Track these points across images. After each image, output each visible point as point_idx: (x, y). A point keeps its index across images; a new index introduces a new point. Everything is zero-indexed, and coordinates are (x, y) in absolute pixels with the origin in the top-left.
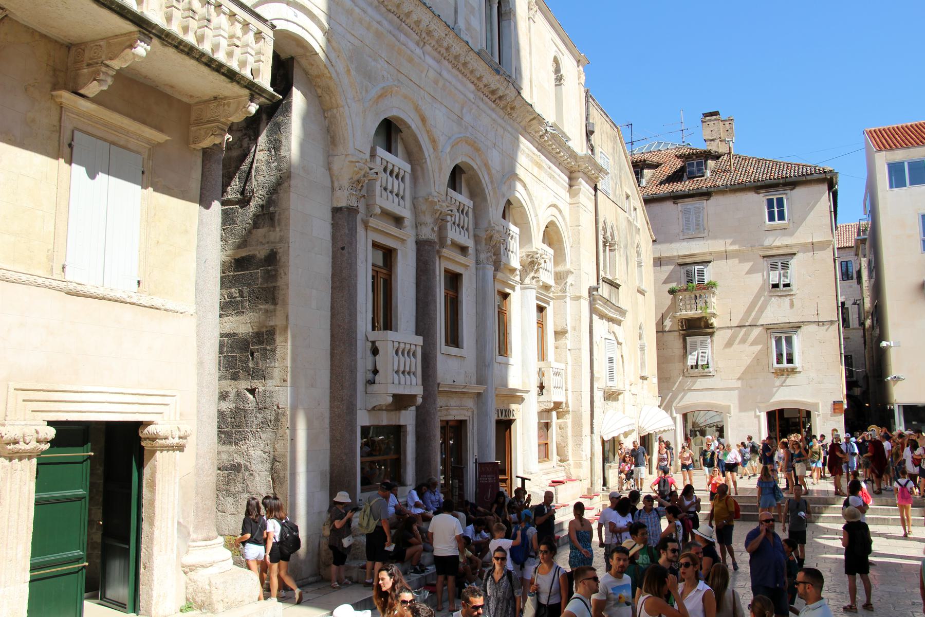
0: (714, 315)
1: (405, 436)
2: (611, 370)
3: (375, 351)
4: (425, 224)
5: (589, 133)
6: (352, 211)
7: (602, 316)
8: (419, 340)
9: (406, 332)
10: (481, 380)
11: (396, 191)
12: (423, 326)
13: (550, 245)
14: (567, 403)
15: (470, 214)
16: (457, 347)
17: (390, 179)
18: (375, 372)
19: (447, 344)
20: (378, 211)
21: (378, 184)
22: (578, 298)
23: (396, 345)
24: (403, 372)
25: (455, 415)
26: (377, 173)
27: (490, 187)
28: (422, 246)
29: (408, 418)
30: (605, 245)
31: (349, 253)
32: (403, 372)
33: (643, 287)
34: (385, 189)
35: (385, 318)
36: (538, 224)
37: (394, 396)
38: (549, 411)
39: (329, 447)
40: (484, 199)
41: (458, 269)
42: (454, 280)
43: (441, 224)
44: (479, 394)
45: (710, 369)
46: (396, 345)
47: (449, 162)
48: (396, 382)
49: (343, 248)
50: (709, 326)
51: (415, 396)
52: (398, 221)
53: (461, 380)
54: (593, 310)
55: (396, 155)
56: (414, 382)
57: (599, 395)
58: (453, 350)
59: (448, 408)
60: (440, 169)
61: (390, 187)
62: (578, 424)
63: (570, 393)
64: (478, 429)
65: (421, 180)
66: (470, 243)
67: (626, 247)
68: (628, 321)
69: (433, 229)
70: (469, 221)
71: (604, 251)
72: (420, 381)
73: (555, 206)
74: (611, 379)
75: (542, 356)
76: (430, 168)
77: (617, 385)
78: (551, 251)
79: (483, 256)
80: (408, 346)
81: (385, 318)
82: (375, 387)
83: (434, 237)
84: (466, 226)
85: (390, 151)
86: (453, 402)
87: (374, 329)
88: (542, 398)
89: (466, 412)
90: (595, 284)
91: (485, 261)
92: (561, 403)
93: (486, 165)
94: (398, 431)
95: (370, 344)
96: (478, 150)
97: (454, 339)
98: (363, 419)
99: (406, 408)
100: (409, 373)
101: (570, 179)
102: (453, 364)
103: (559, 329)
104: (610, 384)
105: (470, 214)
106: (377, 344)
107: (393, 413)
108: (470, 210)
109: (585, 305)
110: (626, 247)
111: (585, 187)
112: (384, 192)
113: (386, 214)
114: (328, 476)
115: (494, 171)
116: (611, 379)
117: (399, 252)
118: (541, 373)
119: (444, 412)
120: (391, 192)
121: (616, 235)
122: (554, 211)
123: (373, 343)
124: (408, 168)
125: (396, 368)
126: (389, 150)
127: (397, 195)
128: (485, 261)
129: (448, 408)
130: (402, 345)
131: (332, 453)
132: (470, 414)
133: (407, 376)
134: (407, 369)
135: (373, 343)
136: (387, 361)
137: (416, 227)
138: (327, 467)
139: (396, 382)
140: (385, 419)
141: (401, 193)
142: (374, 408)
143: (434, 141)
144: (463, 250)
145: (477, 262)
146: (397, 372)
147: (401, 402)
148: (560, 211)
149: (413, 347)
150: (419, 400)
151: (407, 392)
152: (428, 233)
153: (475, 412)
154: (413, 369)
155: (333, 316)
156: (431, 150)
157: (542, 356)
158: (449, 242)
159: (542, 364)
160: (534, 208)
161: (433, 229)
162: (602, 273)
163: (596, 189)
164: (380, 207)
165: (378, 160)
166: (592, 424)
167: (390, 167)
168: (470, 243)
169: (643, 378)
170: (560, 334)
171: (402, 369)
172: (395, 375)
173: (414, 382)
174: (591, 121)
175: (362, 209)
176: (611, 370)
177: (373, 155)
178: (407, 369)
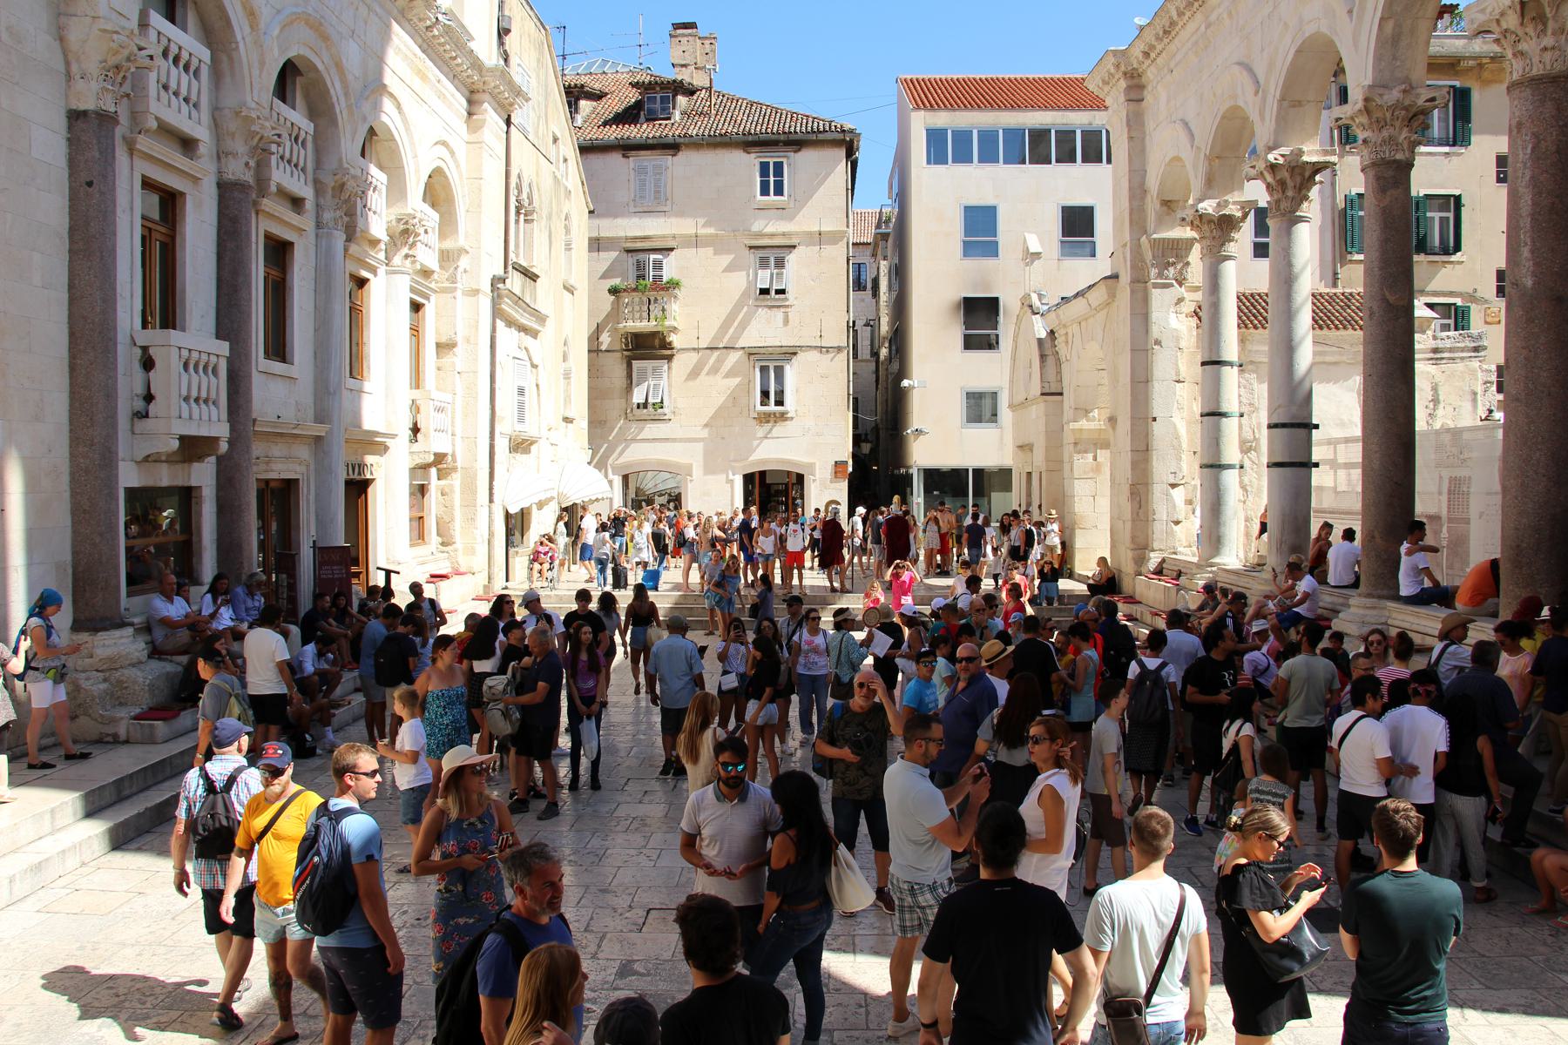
0: (674, 330)
1: (199, 504)
2: (521, 407)
3: (148, 364)
4: (235, 155)
5: (503, 32)
6: (105, 120)
7: (510, 323)
8: (224, 348)
9: (198, 332)
10: (321, 417)
11: (184, 92)
12: (229, 324)
13: (433, 206)
14: (453, 456)
15: (310, 145)
16: (283, 360)
17: (173, 69)
18: (149, 398)
19: (267, 355)
20: (154, 125)
21: (153, 76)
22: (476, 292)
23: (185, 353)
24: (197, 400)
25: (280, 471)
26: (151, 57)
27: (343, 104)
28: (228, 191)
29: (203, 475)
30: (518, 213)
31: (102, 193)
32: (197, 400)
33: (572, 282)
34: (166, 87)
35: (164, 308)
36: (417, 171)
37: (182, 438)
38: (425, 467)
39: (69, 522)
40: (333, 122)
41: (287, 235)
42: (279, 252)
43: (261, 154)
44: (318, 439)
45: (665, 410)
46: (185, 353)
47: (276, 52)
48: (185, 414)
49: (90, 184)
50: (666, 345)
51: (217, 439)
52: (188, 145)
53: (289, 415)
54: (497, 313)
55: (185, 30)
56: (214, 418)
57: (502, 445)
58: (277, 367)
59: (269, 460)
60: (262, 63)
61: (173, 85)
62: (469, 488)
63: (458, 439)
64: (317, 495)
65: (228, 79)
66: (307, 192)
67: (550, 217)
68: (548, 331)
69: (247, 164)
70: (306, 156)
71: (517, 222)
72: (224, 416)
73: (444, 143)
74: (521, 420)
75: (417, 380)
76: (244, 60)
77: (530, 429)
78: (435, 216)
79: (327, 216)
80: (204, 357)
81: (164, 308)
82: (148, 424)
83: (249, 177)
84: (301, 164)
85: (173, 21)
86: (277, 450)
87: (144, 326)
88: (416, 447)
89: (298, 468)
90: (500, 272)
91: (331, 224)
92: (445, 455)
93: (339, 66)
94: (186, 497)
95: (139, 352)
96: (325, 38)
97: (278, 348)
98: (129, 476)
99: (200, 458)
100: (206, 401)
101: (470, 102)
102: (277, 389)
103: (443, 340)
104: (519, 427)
105: (310, 145)
106: (151, 351)
107: (179, 466)
108: (310, 138)
109: (485, 303)
110: (550, 217)
111: (491, 118)
112: (162, 92)
113: (167, 131)
114: (70, 571)
115: (350, 78)
116: (521, 420)
117: (189, 198)
118: (415, 407)
119: (263, 467)
120: (176, 94)
121: (535, 197)
122: (442, 151)
123: (145, 349)
124: (205, 54)
125: (184, 393)
126: (171, 18)
127: (186, 100)
128: (331, 224)
129: (269, 460)
130: (195, 355)
131: (75, 532)
132: (303, 469)
133: (203, 406)
134: (204, 395)
135: (145, 349)
136: (170, 380)
137: (219, 158)
138: (67, 557)
139: (185, 414)
140: (165, 477)
141: (194, 97)
142: (146, 459)
143: (251, 14)
144: (297, 203)
145: (319, 225)
146: (187, 399)
147: (193, 448)
148: (452, 153)
149: (213, 359)
150: (224, 447)
151: (204, 432)
152: (238, 170)
153: (312, 467)
154: (213, 395)
155: (72, 301)
156: (247, 30)
157: (417, 380)
158: (273, 188)
159: (416, 394)
160: (412, 144)
161: (247, 164)
162: (512, 256)
163: (508, 122)
164: (157, 119)
165: (153, 36)
166: (491, 489)
167: (174, 50)
168: (307, 192)
169: (567, 420)
170: (444, 347)
171: (194, 394)
172: (184, 405)
173: (214, 418)
174: (507, 13)
175: (124, 119)
176: (521, 407)
177: (144, 25)
178: (204, 395)
